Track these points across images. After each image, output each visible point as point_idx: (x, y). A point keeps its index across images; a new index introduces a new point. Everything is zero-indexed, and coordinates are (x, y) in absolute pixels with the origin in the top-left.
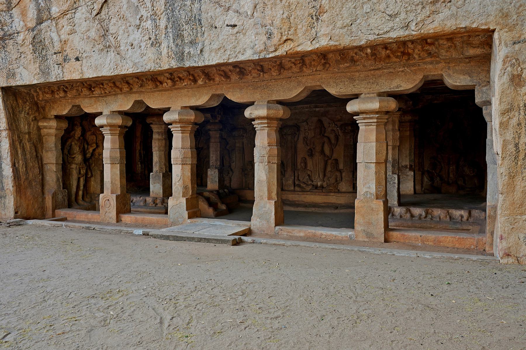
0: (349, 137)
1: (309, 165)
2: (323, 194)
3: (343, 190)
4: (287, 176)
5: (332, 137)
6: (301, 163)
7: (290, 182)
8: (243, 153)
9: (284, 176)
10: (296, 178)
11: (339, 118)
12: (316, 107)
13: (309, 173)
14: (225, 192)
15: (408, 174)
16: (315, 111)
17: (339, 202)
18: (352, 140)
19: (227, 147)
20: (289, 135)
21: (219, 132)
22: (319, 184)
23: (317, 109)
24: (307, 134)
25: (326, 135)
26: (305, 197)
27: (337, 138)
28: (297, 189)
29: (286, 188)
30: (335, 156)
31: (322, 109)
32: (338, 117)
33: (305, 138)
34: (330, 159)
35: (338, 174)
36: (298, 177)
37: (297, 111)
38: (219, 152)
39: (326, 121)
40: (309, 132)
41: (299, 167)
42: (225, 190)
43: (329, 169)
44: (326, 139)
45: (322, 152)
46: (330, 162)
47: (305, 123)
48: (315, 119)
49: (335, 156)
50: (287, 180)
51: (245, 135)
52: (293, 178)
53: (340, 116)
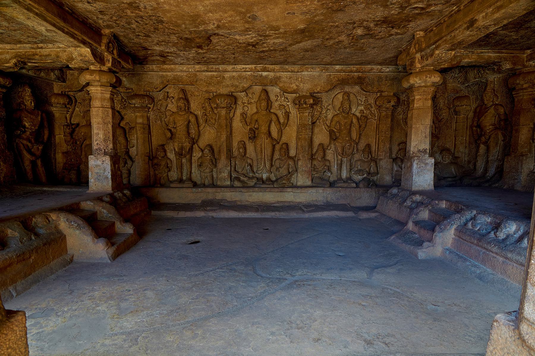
0: (307, 114)
1: (248, 151)
2: (277, 190)
3: (299, 184)
4: (220, 165)
5: (280, 114)
6: (239, 149)
7: (225, 174)
8: (150, 133)
9: (216, 166)
10: (233, 169)
11: (295, 87)
12: (264, 70)
13: (249, 161)
14: (124, 195)
15: (427, 161)
16: (261, 76)
17: (298, 200)
18: (310, 118)
19: (122, 125)
20: (223, 108)
21: (110, 89)
22: (265, 176)
23: (265, 74)
24: (246, 109)
25: (272, 111)
26: (250, 196)
27: (287, 115)
28: (237, 184)
29: (219, 183)
30: (284, 139)
31: (272, 74)
32: (294, 86)
33: (244, 115)
34: (278, 143)
35: (291, 163)
36: (235, 168)
37: (234, 74)
38: (110, 126)
39: (274, 91)
40: (249, 106)
41: (236, 153)
42: (125, 192)
43: (277, 156)
44: (274, 118)
45: (269, 134)
46: (278, 147)
47: (243, 93)
48: (258, 89)
49: (284, 139)
50: (220, 172)
51: (151, 106)
52: (229, 168)
53: (297, 86)
